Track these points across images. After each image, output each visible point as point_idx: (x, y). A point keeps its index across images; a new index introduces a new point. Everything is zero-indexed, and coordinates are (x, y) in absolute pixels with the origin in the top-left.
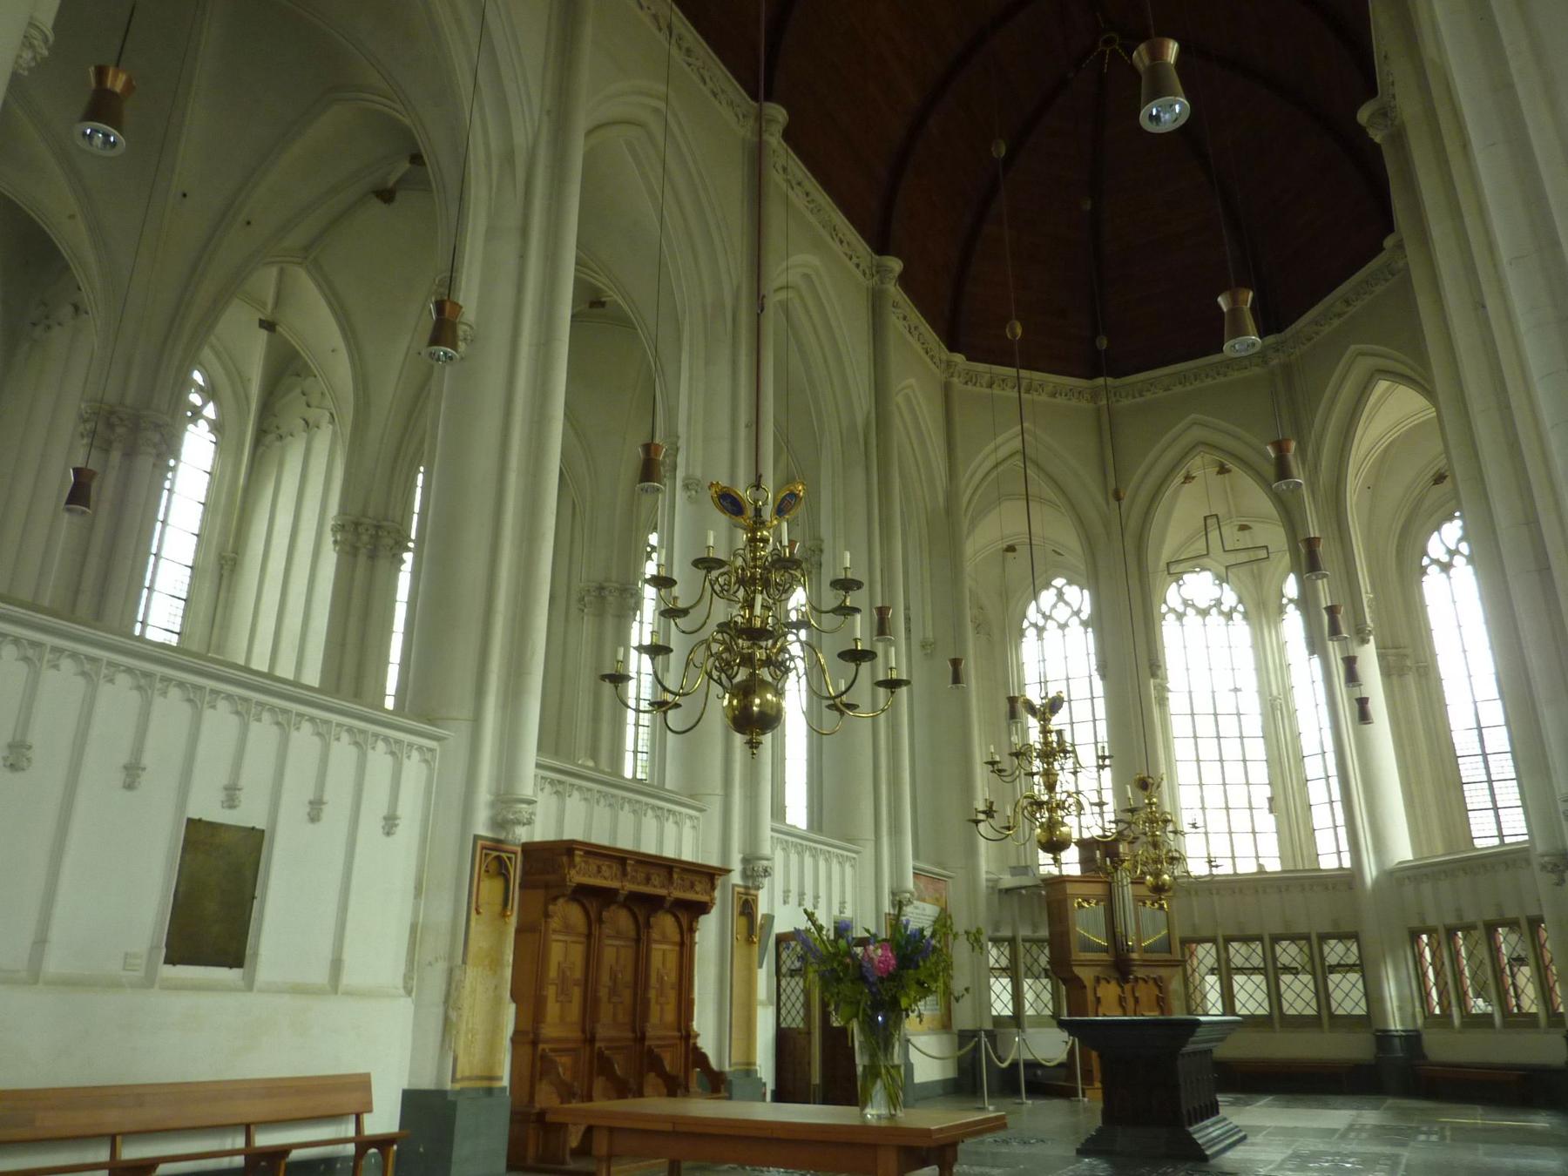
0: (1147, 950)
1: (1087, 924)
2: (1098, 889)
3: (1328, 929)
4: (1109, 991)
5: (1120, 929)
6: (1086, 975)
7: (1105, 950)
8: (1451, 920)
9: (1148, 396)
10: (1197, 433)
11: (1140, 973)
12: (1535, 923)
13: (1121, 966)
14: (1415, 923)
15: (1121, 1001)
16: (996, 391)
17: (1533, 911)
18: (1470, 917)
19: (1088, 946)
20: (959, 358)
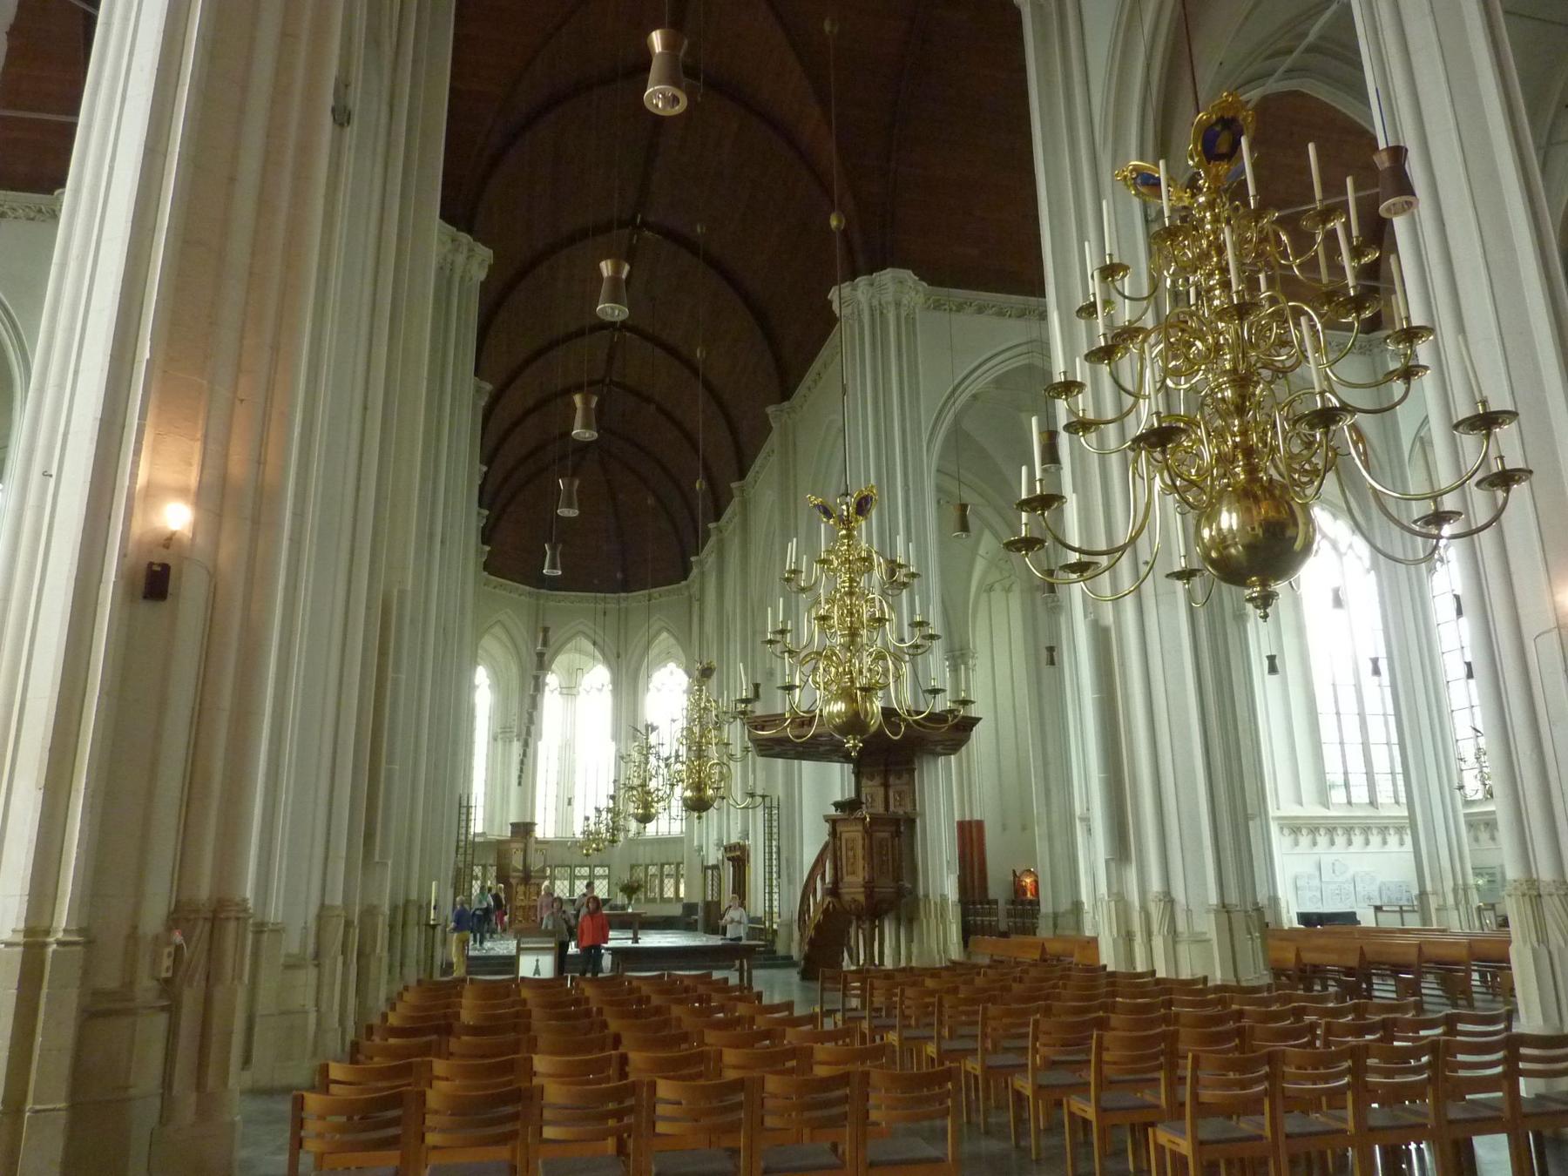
0: (537, 871)
1: (517, 861)
2: (521, 845)
3: (598, 863)
4: (521, 889)
5: (528, 861)
6: (513, 881)
7: (518, 871)
8: (648, 862)
9: (562, 604)
10: (581, 627)
11: (533, 881)
12: (678, 865)
13: (527, 878)
14: (634, 862)
15: (525, 894)
16: (497, 591)
17: (679, 860)
18: (655, 862)
19: (517, 870)
20: (486, 573)
